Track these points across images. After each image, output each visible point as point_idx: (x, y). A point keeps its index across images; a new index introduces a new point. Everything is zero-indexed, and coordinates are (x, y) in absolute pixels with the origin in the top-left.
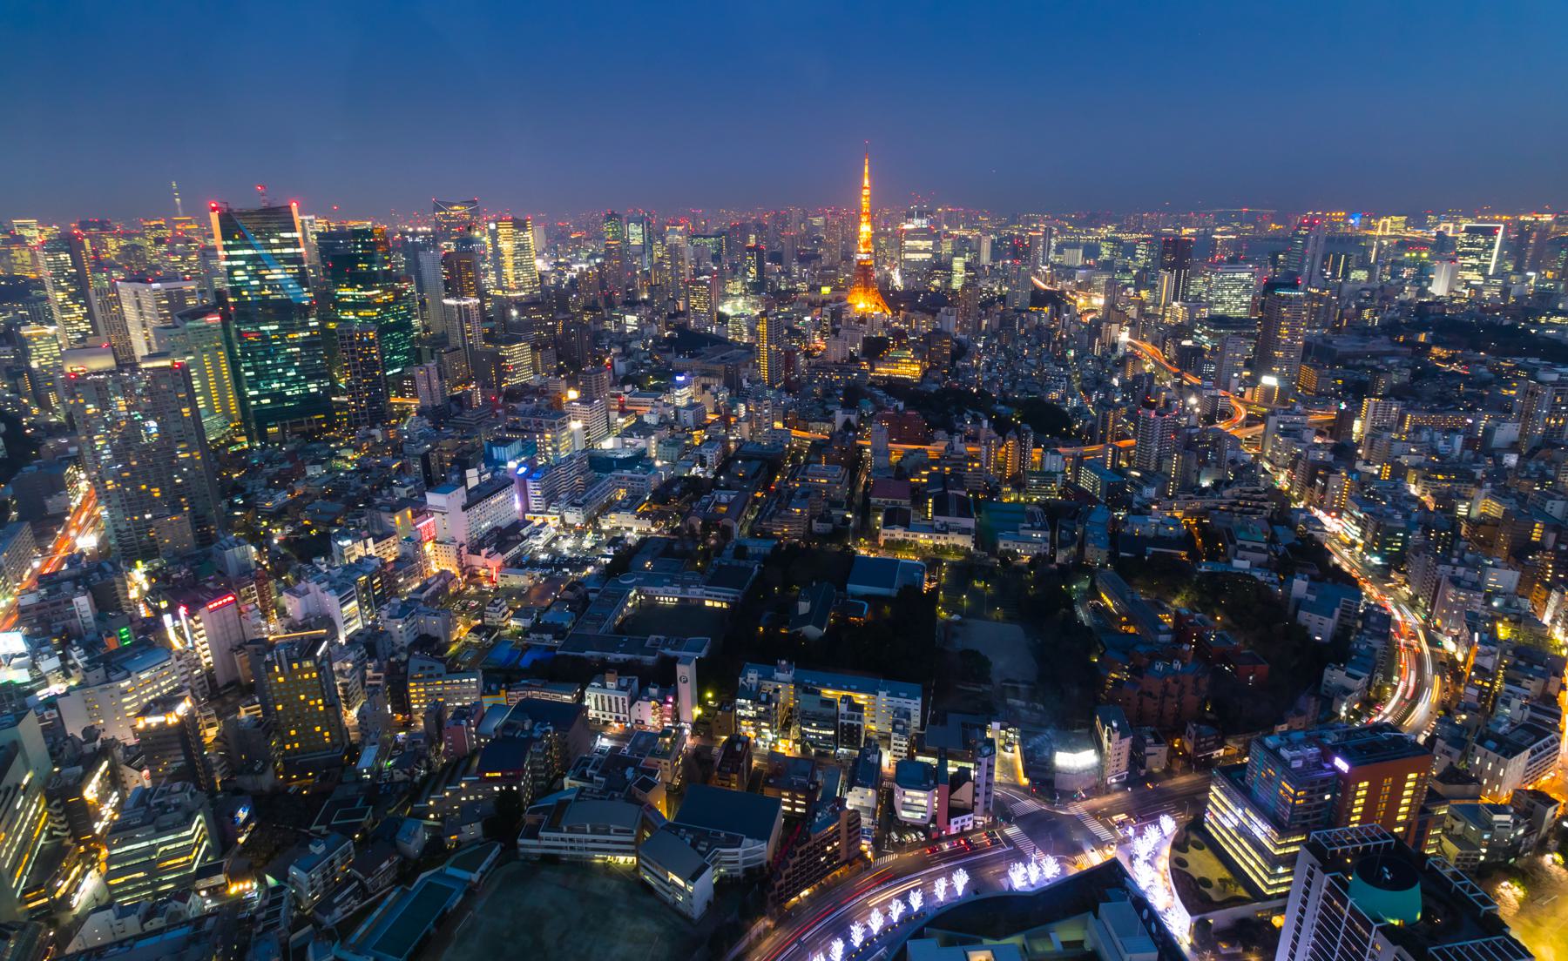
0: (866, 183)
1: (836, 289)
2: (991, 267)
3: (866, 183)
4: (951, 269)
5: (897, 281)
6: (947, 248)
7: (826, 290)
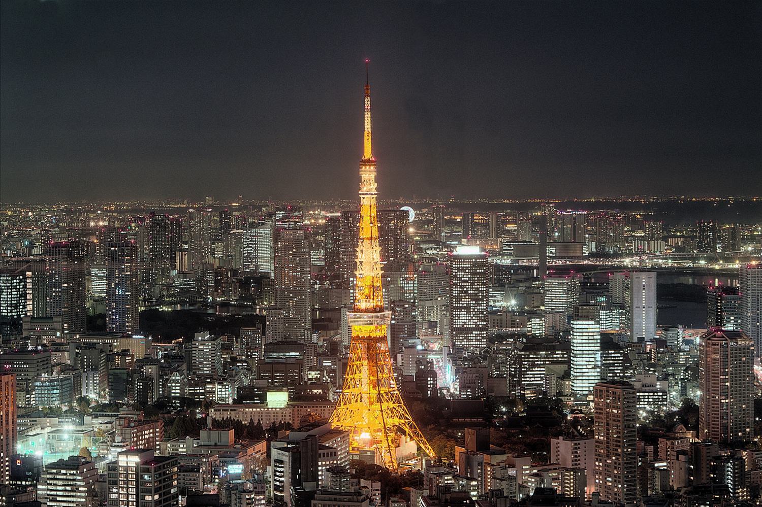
0: (368, 153)
1: (300, 395)
2: (660, 343)
3: (368, 153)
4: (566, 346)
5: (448, 380)
6: (558, 295)
7: (278, 399)
